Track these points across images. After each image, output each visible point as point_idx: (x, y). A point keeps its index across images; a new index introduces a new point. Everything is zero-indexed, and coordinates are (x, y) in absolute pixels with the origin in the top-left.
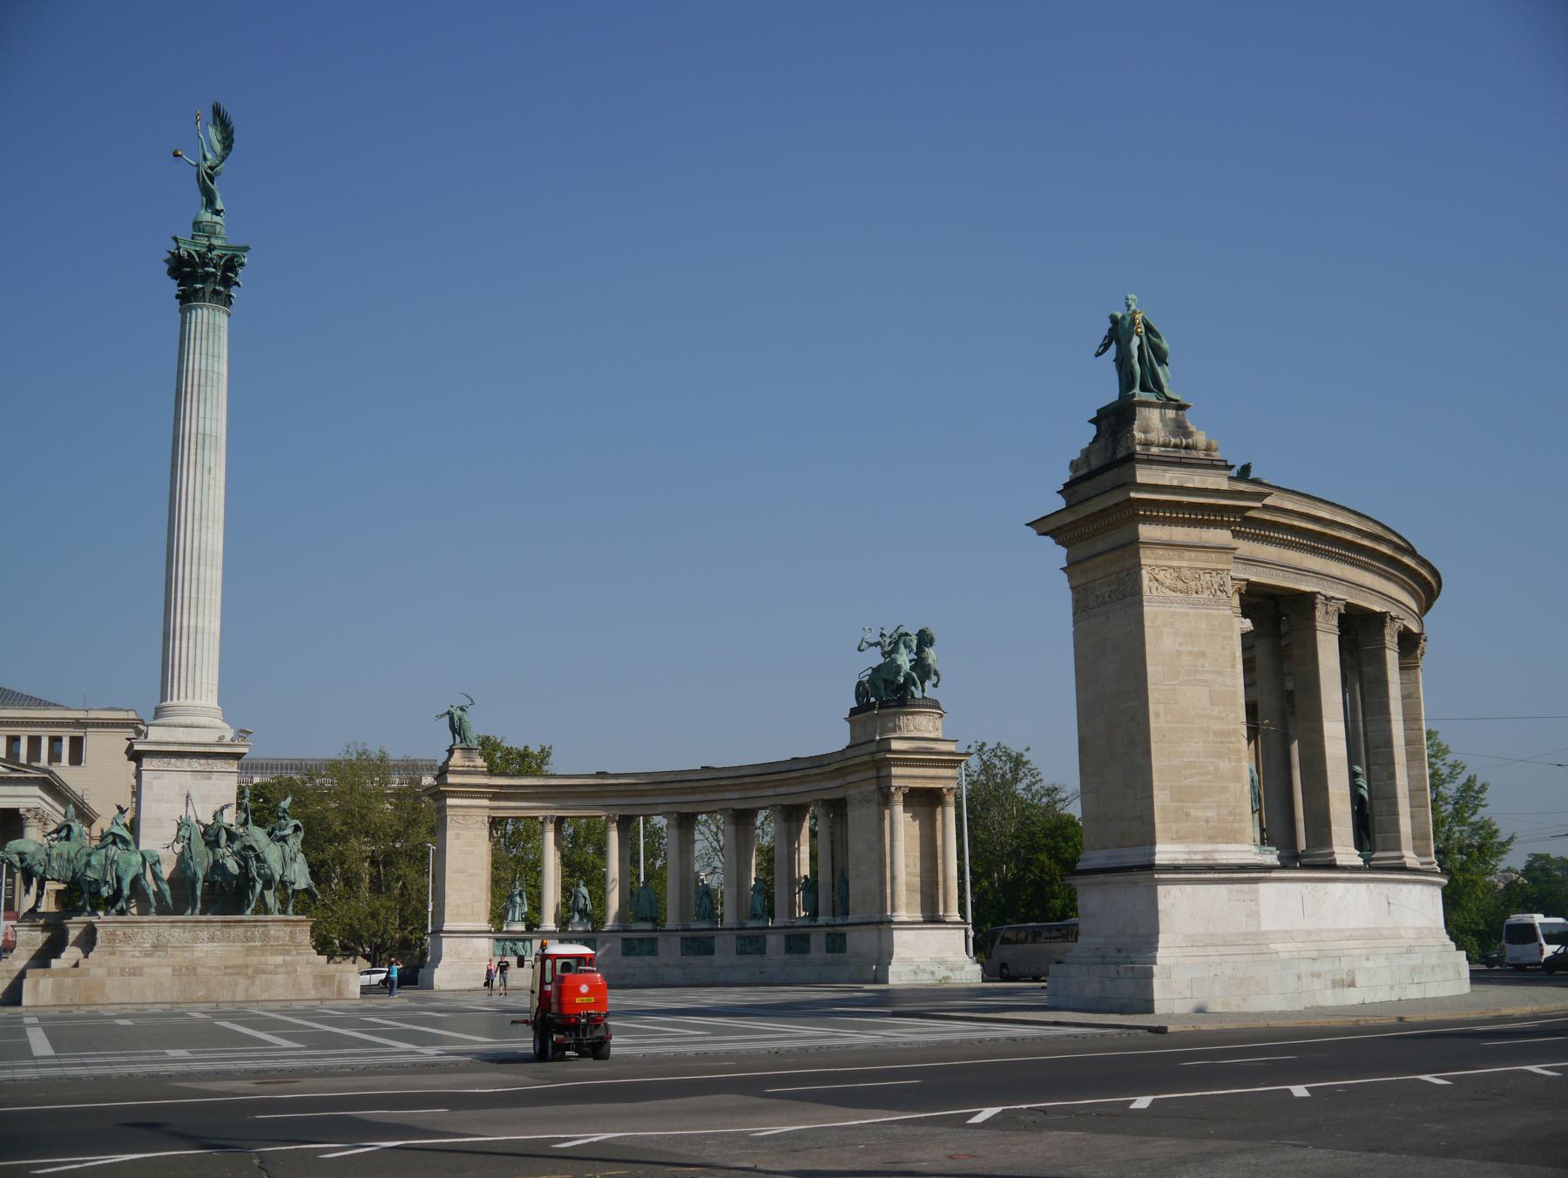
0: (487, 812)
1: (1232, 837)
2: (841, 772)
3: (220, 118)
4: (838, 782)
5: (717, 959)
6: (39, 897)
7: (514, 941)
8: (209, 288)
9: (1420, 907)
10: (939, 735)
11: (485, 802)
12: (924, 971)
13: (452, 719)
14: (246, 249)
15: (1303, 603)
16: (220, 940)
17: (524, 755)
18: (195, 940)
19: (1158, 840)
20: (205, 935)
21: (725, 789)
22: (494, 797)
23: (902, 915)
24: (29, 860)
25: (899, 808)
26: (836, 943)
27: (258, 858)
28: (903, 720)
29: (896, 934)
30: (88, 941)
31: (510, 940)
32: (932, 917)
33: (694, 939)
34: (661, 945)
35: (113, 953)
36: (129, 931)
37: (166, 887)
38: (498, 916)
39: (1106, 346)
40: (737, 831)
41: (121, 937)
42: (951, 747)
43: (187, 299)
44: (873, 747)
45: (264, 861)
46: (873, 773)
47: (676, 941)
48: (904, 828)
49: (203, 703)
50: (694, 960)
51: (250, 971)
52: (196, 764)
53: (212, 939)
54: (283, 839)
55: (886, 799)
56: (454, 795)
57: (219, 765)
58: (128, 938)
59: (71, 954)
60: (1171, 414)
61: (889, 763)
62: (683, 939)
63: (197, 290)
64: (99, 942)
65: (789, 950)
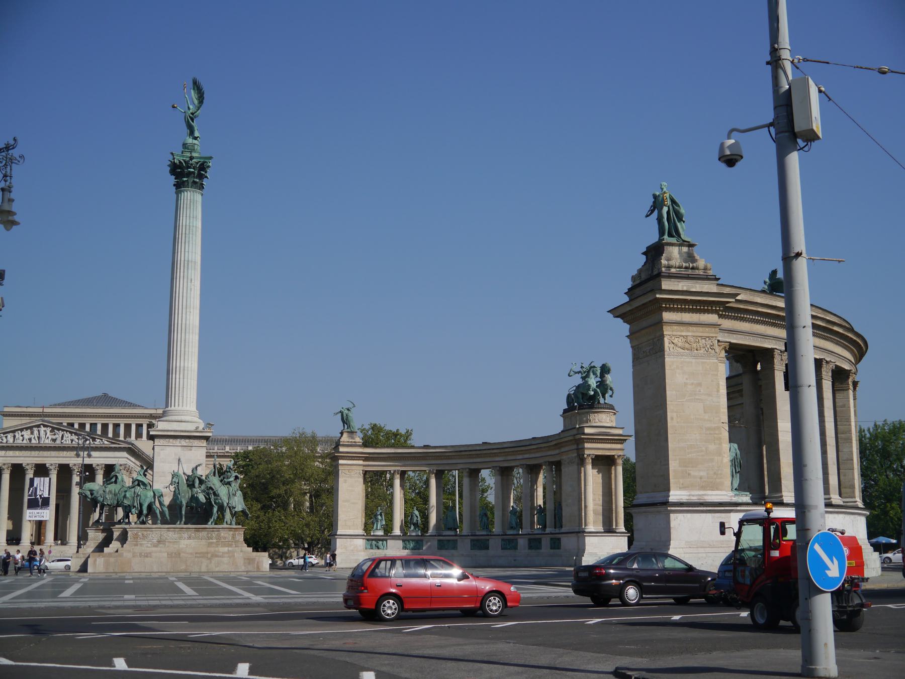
0: (362, 468)
1: (715, 487)
2: (558, 446)
3: (197, 86)
4: (557, 452)
5: (491, 552)
6: (101, 514)
8: (191, 180)
11: (361, 462)
13: (342, 415)
14: (211, 158)
15: (96, 424)
16: (194, 538)
17: (396, 435)
18: (180, 538)
19: (671, 488)
20: (186, 535)
21: (495, 455)
22: (366, 459)
23: (591, 528)
24: (95, 494)
25: (589, 466)
26: (556, 544)
27: (215, 494)
28: (592, 416)
29: (587, 539)
30: (123, 538)
31: (375, 540)
32: (609, 530)
33: (477, 540)
34: (459, 544)
35: (136, 545)
36: (145, 533)
37: (166, 510)
38: (368, 528)
39: (652, 211)
40: (502, 479)
41: (141, 536)
42: (620, 432)
43: (179, 186)
44: (574, 432)
45: (218, 496)
46: (575, 447)
47: (467, 542)
48: (592, 478)
49: (188, 408)
50: (478, 553)
51: (209, 556)
52: (184, 442)
53: (189, 538)
54: (229, 483)
55: (582, 461)
56: (343, 458)
57: (196, 442)
58: (144, 537)
59: (115, 545)
60: (685, 249)
61: (583, 441)
62: (472, 540)
63: (184, 182)
64: (129, 539)
65: (530, 548)
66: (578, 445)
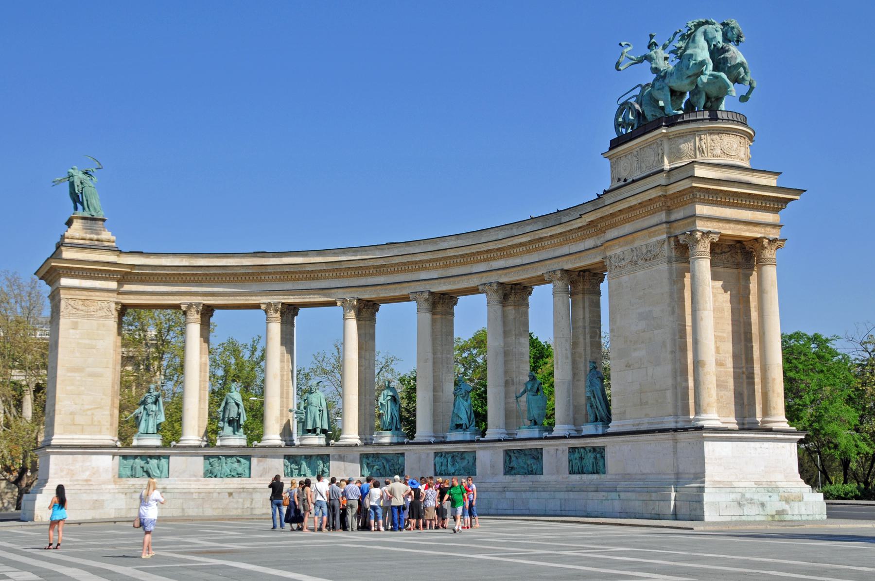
0: (114, 297)
4: (589, 243)
7: (146, 458)
9: (784, 455)
10: (746, 164)
11: (113, 285)
12: (751, 502)
21: (421, 265)
26: (588, 461)
28: (707, 141)
29: (708, 446)
31: (141, 457)
32: (749, 426)
33: (376, 456)
38: (127, 429)
42: (772, 181)
46: (662, 216)
55: (683, 251)
56: (71, 273)
65: (509, 470)
66: (669, 211)
